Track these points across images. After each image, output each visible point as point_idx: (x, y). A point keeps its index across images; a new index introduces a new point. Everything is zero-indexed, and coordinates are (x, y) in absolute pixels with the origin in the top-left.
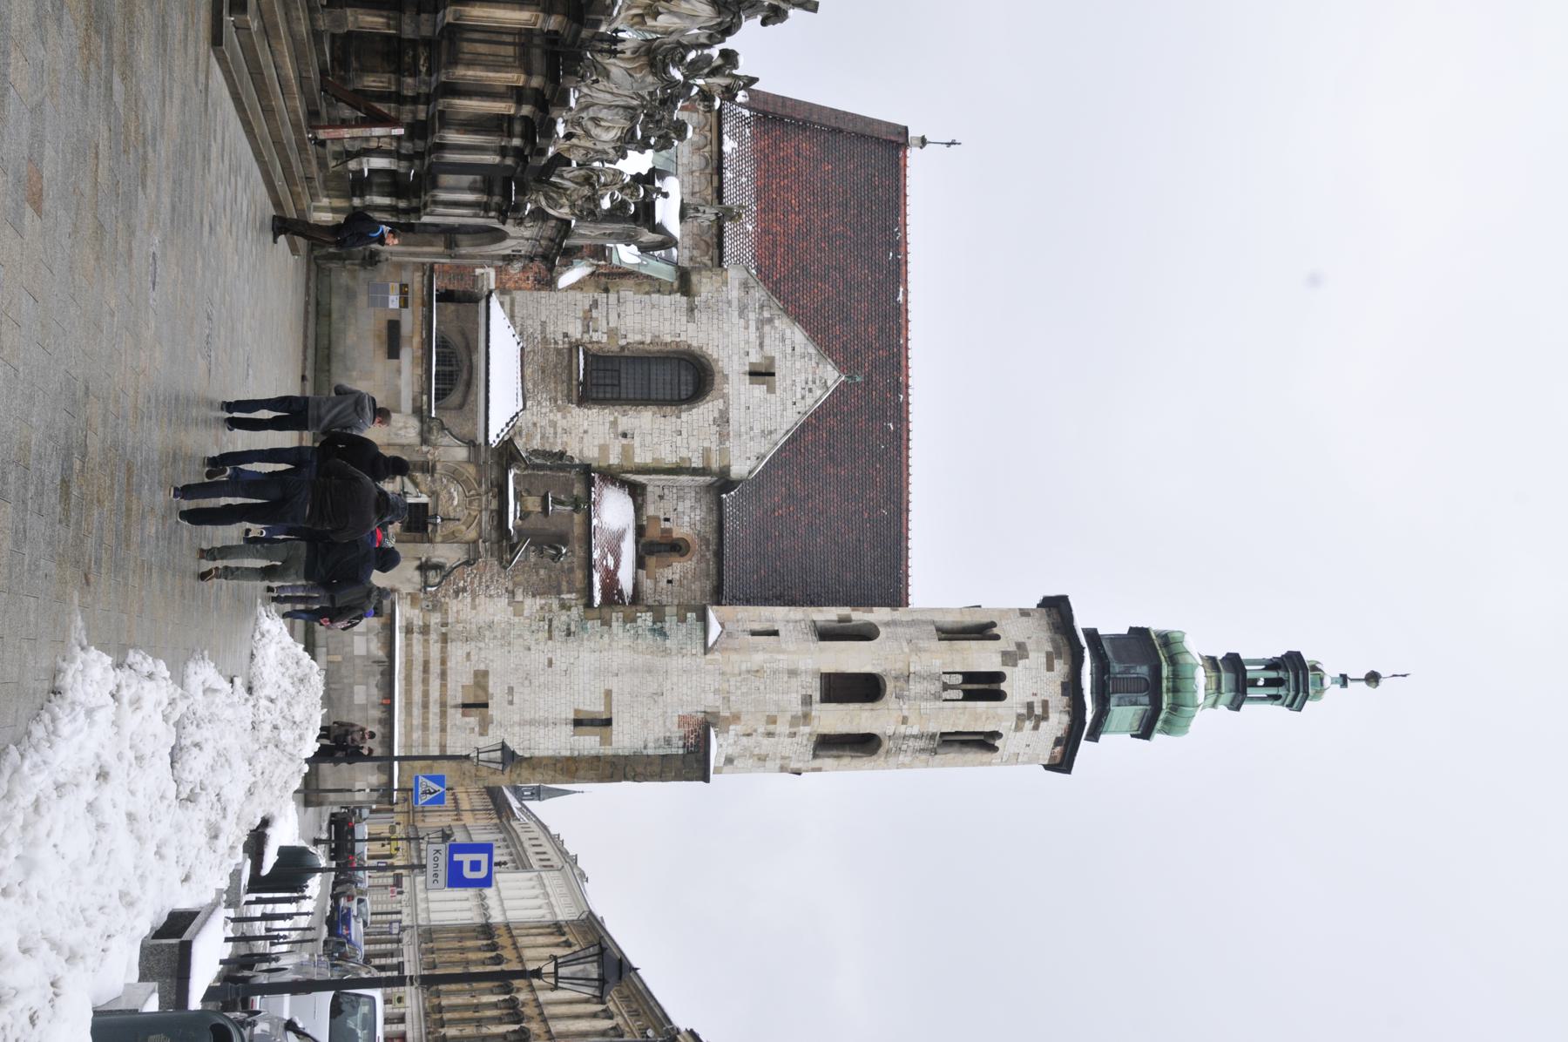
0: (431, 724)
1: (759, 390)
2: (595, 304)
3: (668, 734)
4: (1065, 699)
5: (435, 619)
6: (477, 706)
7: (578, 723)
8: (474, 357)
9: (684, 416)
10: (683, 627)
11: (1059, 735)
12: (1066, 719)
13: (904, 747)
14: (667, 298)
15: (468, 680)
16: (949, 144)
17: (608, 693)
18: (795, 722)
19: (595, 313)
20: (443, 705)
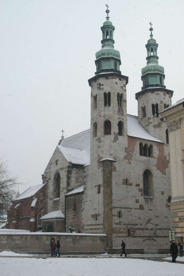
0: (99, 228)
1: (59, 163)
2: (49, 198)
3: (101, 171)
4: (97, 81)
5: (86, 227)
6: (95, 217)
7: (99, 192)
8: (48, 222)
9: (61, 177)
10: (86, 171)
11: (105, 79)
12: (100, 79)
13: (108, 114)
14: (49, 184)
15: (92, 220)
16: (63, 131)
17: (95, 186)
18: (100, 142)
19: (50, 198)
20: (96, 225)
